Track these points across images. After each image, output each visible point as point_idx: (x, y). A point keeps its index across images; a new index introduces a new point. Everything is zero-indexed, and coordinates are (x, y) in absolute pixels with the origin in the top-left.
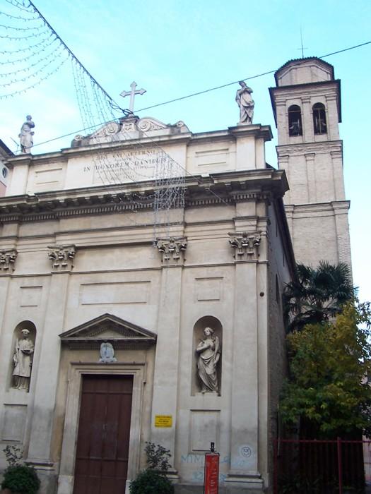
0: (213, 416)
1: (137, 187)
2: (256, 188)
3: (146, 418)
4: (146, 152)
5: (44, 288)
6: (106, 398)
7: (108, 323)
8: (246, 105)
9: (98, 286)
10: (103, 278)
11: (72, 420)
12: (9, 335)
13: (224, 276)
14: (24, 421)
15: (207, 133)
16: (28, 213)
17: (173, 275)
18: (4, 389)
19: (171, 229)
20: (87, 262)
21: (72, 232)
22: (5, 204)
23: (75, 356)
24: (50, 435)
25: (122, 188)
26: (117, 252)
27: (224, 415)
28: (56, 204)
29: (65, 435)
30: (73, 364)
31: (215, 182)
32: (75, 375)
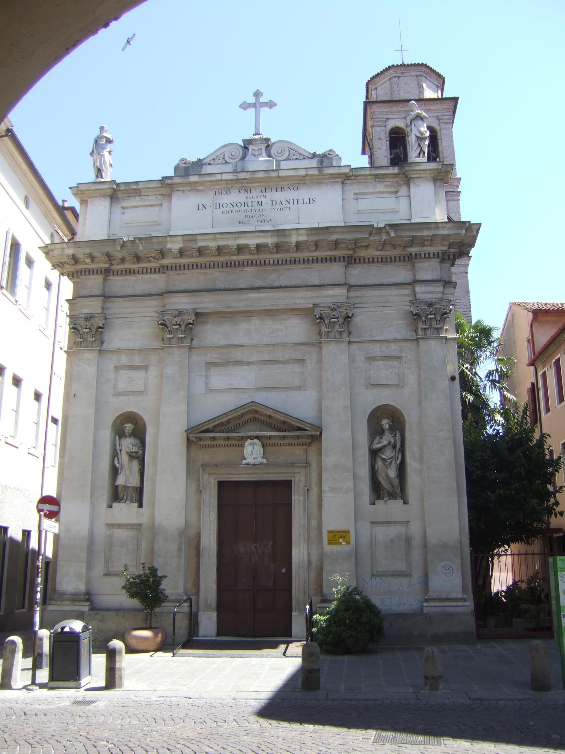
0: (401, 529)
3: (314, 533)
5: (151, 368)
8: (419, 135)
11: (210, 540)
13: (403, 354)
14: (138, 545)
17: (335, 354)
18: (104, 505)
20: (212, 334)
24: (183, 561)
27: (415, 528)
29: (202, 560)
32: (210, 482)
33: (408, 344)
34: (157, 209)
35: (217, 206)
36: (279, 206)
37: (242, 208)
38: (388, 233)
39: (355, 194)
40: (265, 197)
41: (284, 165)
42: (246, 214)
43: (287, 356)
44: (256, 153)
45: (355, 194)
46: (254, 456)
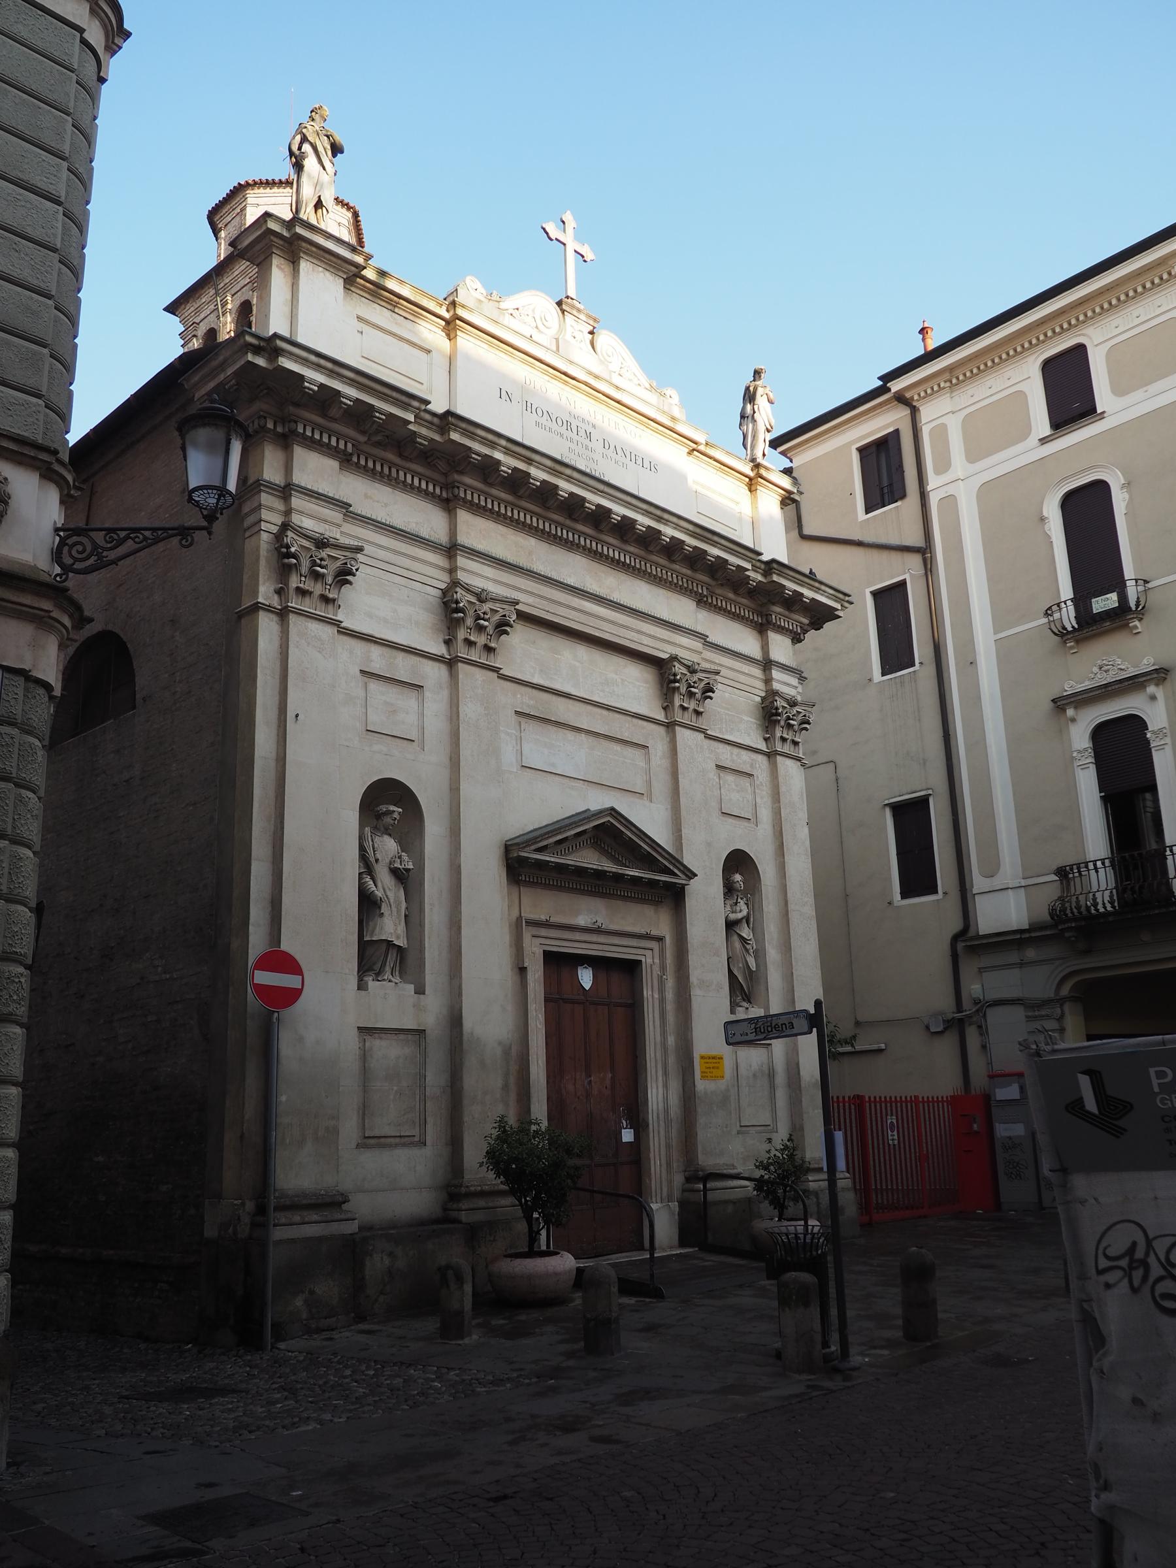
7: (611, 833)
9: (552, 729)
12: (351, 817)
16: (378, 444)
19: (684, 641)
22: (353, 392)
23: (543, 905)
26: (583, 652)
28: (488, 469)
36: (610, 453)
42: (569, 444)
43: (626, 736)
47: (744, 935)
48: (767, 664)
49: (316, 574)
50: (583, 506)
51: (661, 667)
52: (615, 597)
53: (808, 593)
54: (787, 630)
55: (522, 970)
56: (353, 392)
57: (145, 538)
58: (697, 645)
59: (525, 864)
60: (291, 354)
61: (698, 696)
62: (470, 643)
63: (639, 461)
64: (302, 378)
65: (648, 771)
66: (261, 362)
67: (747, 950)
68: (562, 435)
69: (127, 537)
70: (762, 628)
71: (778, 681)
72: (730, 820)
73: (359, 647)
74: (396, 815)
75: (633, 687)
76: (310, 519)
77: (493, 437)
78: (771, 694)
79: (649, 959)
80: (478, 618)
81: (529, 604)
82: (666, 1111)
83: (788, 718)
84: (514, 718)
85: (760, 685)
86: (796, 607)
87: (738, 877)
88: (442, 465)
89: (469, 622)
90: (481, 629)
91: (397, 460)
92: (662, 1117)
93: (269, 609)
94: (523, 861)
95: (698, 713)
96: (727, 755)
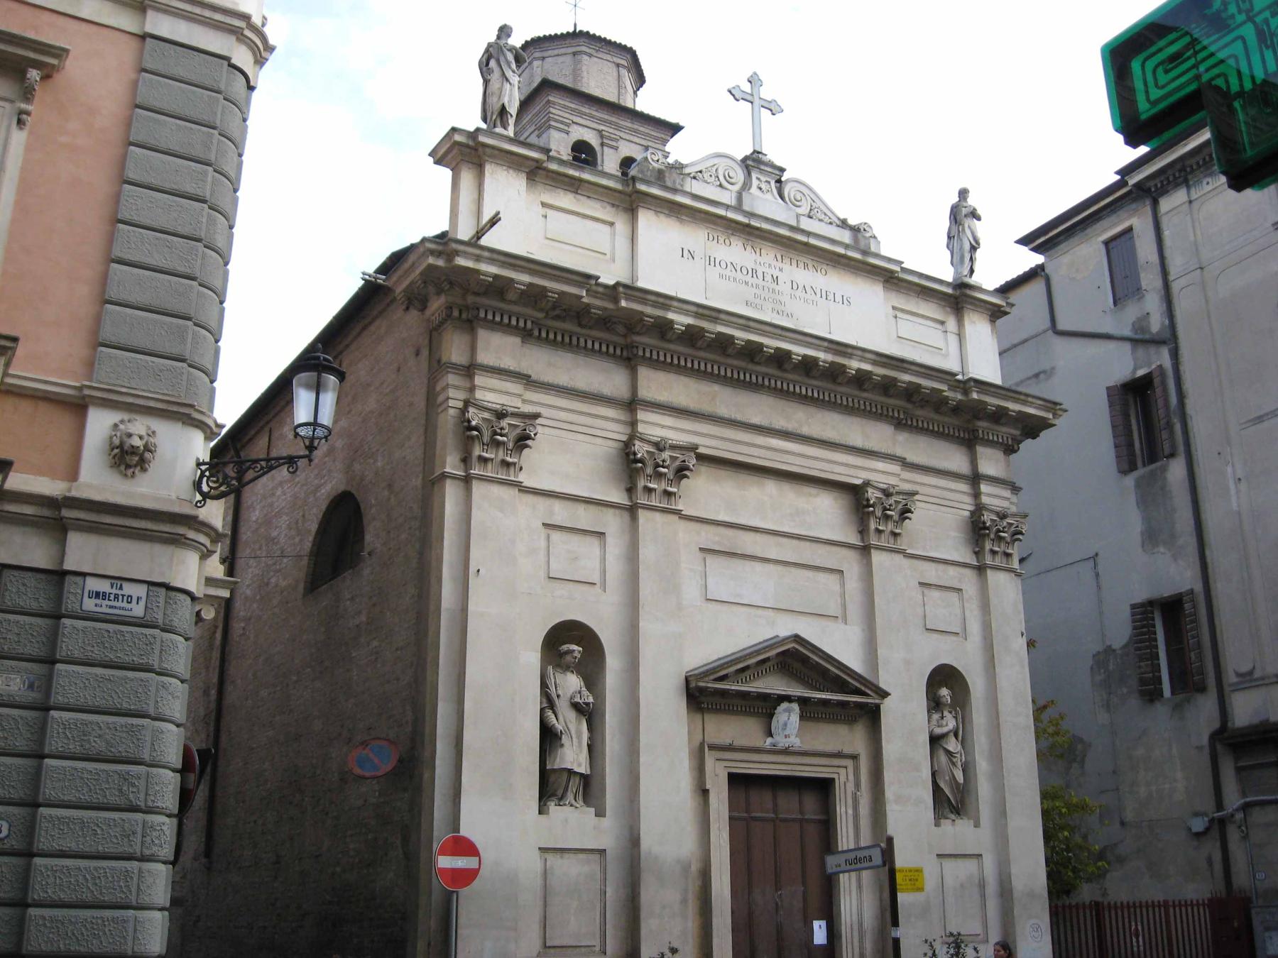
0: (970, 866)
1: (844, 354)
2: (1016, 428)
4: (721, 240)
6: (787, 836)
7: (797, 659)
10: (749, 543)
12: (531, 658)
15: (921, 275)
16: (557, 318)
19: (880, 465)
21: (677, 408)
22: (526, 278)
24: (690, 924)
25: (817, 348)
28: (663, 328)
30: (712, 747)
31: (975, 396)
33: (968, 572)
34: (607, 228)
35: (711, 261)
36: (800, 293)
37: (748, 278)
38: (966, 392)
39: (894, 308)
40: (781, 270)
41: (806, 224)
42: (754, 290)
44: (763, 186)
45: (894, 308)
46: (787, 732)
47: (951, 749)
48: (975, 479)
49: (500, 443)
50: (761, 350)
51: (855, 495)
52: (805, 430)
53: (1013, 406)
54: (997, 443)
55: (705, 793)
56: (526, 278)
57: (262, 468)
58: (895, 468)
59: (705, 694)
60: (465, 253)
61: (896, 517)
62: (649, 491)
63: (831, 297)
64: (477, 272)
65: (843, 595)
66: (440, 263)
67: (954, 764)
68: (747, 283)
69: (249, 468)
70: (969, 442)
71: (989, 495)
72: (935, 636)
73: (542, 503)
74: (576, 654)
75: (825, 515)
76: (492, 393)
77: (665, 301)
78: (979, 509)
79: (844, 779)
80: (657, 465)
81: (708, 446)
82: (861, 924)
83: (999, 531)
84: (700, 555)
85: (969, 500)
86: (1003, 420)
87: (944, 692)
88: (621, 329)
89: (649, 470)
90: (660, 476)
91: (578, 330)
92: (856, 927)
93: (454, 477)
94: (702, 690)
95: (895, 535)
96: (932, 573)
